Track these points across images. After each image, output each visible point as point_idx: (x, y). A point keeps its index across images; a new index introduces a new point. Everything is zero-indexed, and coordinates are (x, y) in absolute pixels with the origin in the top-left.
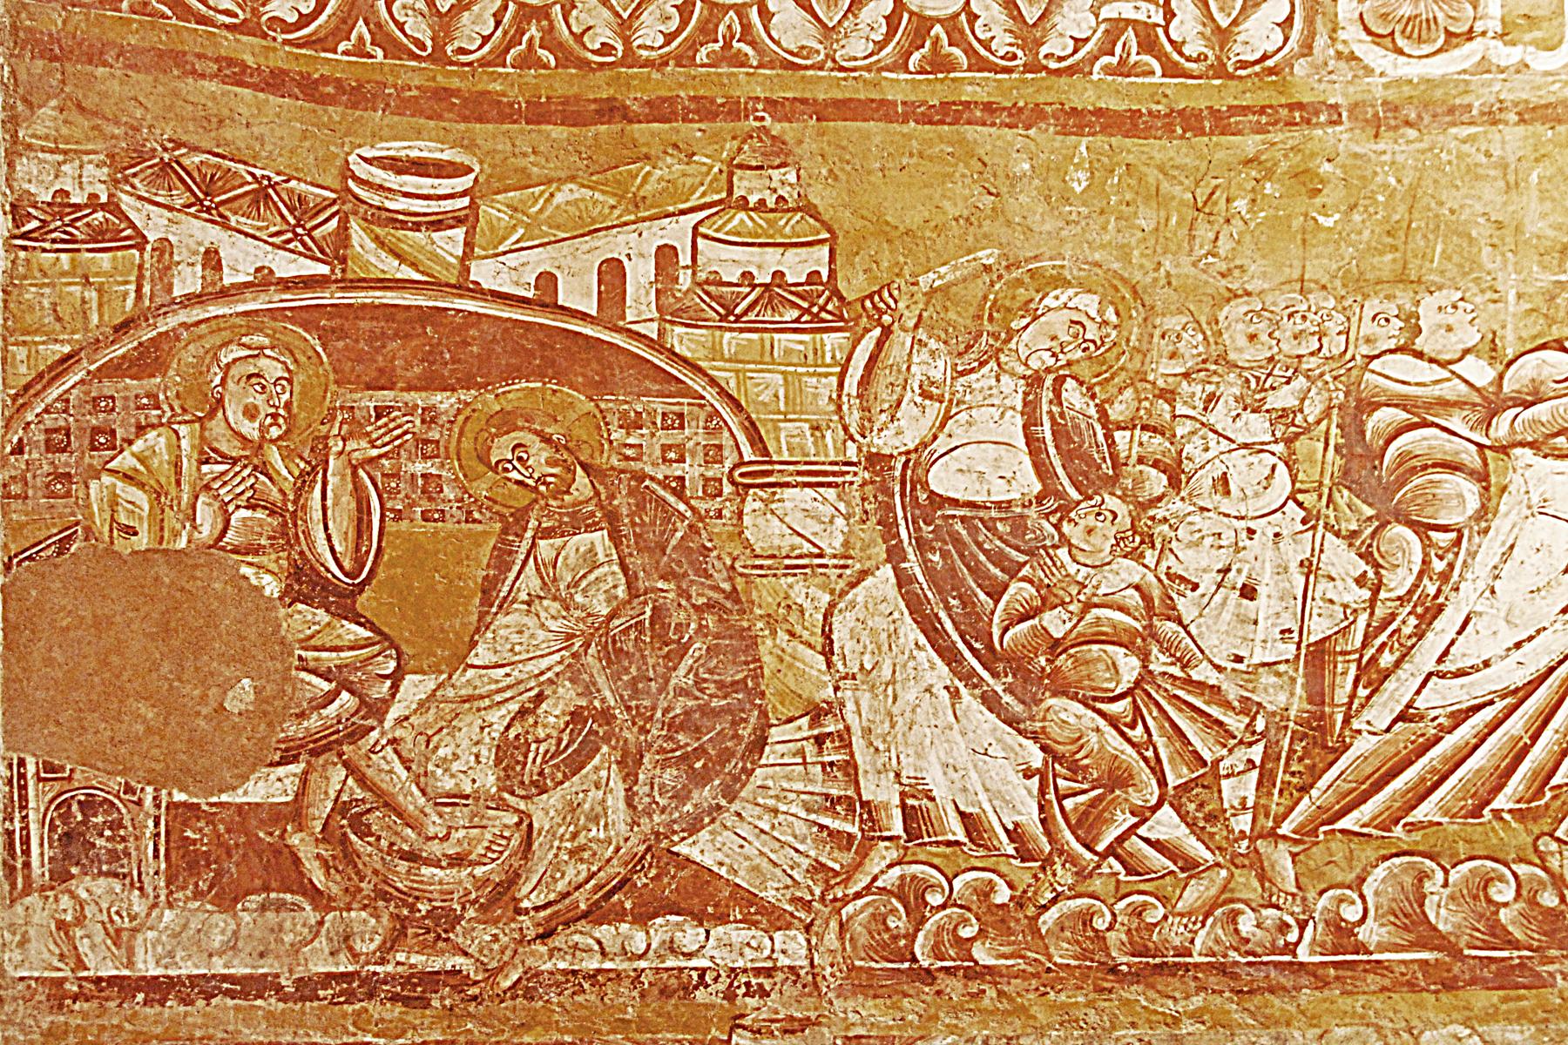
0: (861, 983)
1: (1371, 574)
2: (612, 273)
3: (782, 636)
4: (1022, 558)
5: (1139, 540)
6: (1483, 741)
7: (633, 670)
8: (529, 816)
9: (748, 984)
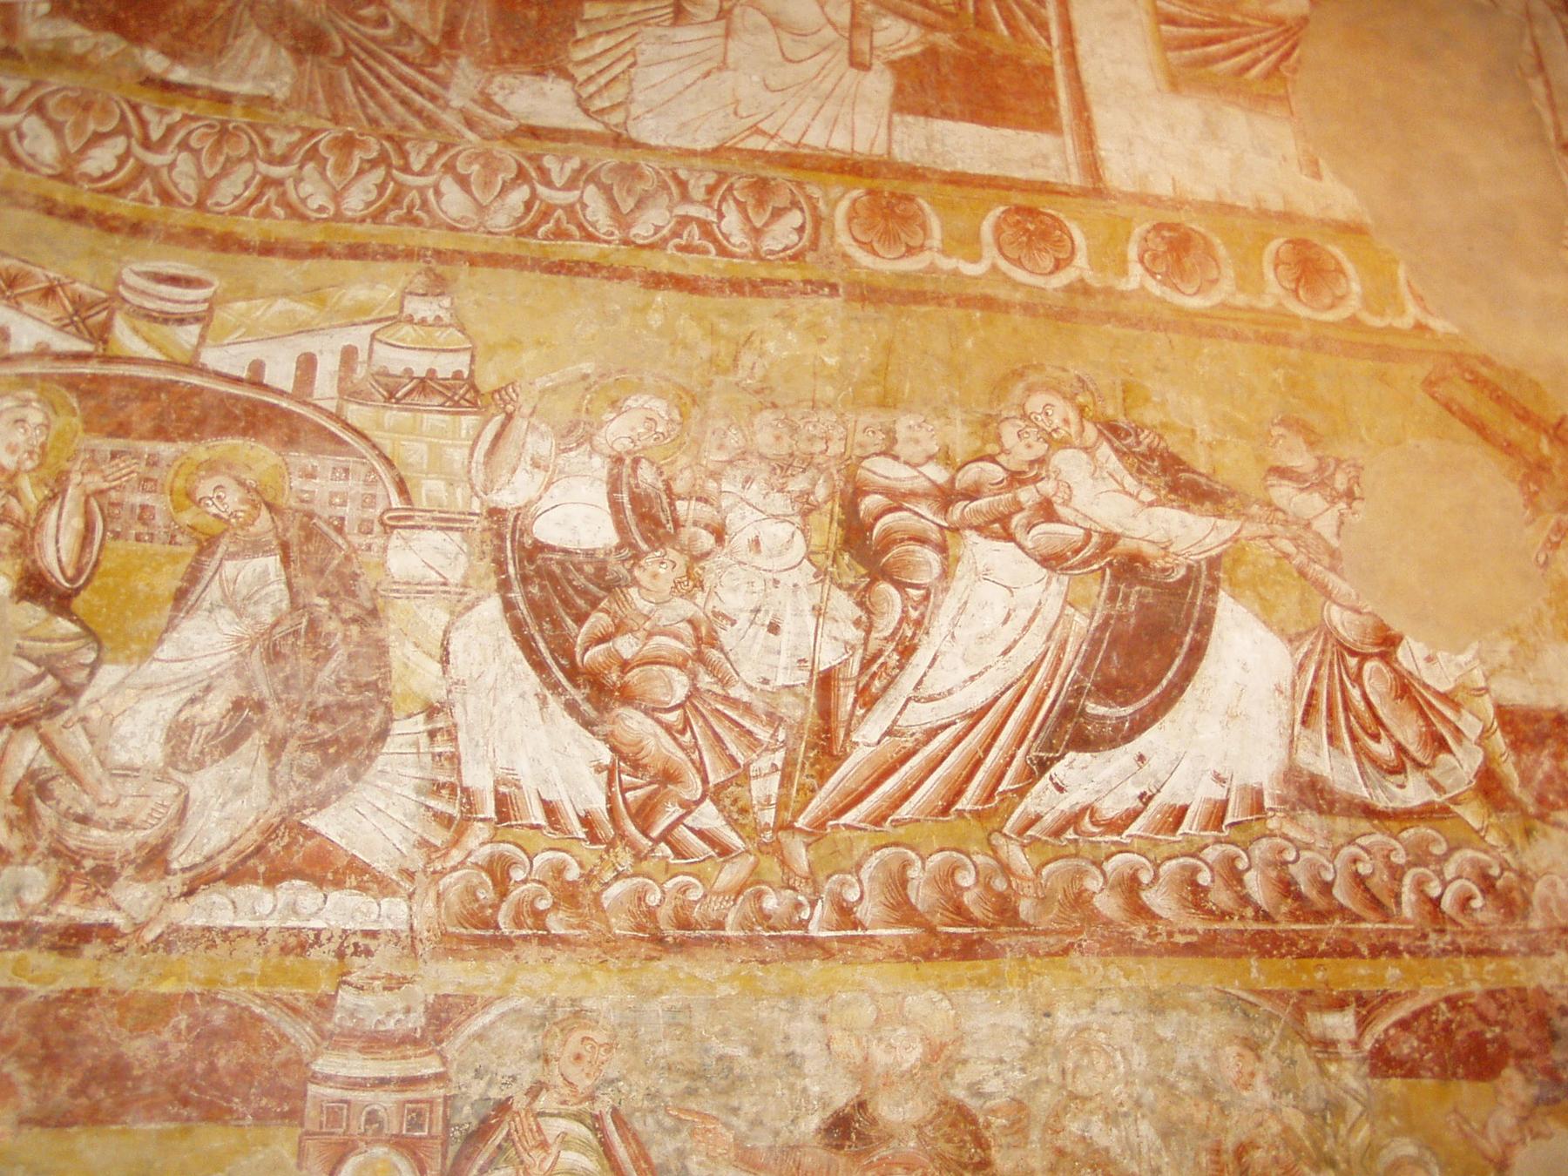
0: (450, 946)
1: (864, 618)
2: (307, 364)
3: (410, 648)
4: (601, 594)
5: (692, 582)
6: (948, 753)
7: (288, 669)
8: (187, 788)
9: (356, 945)
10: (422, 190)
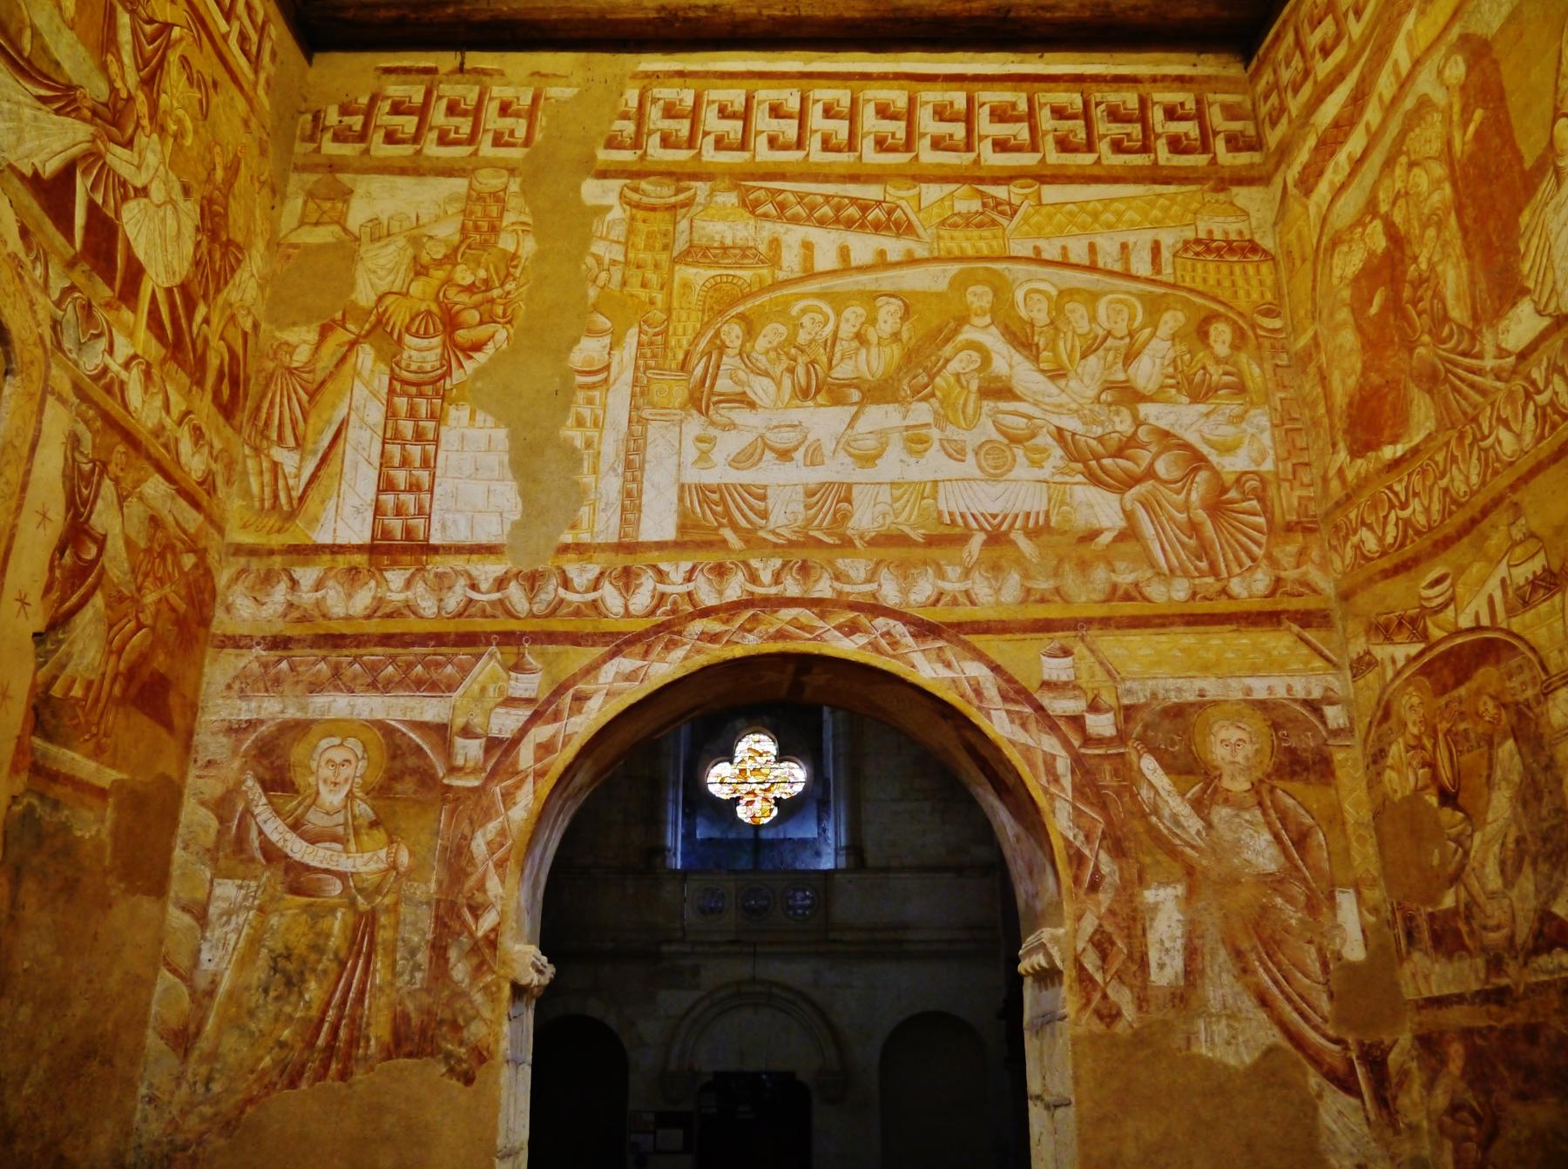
10: (1492, 447)
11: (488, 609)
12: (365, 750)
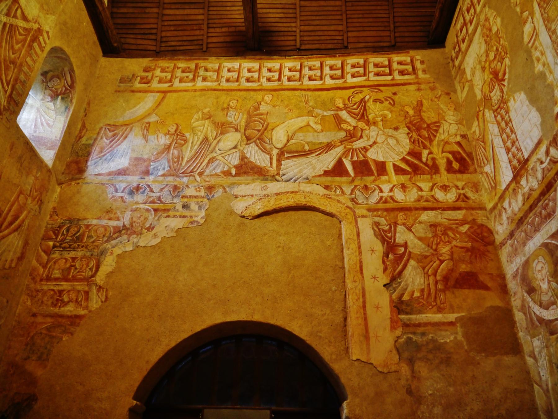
11: (549, 167)
12: (545, 259)
